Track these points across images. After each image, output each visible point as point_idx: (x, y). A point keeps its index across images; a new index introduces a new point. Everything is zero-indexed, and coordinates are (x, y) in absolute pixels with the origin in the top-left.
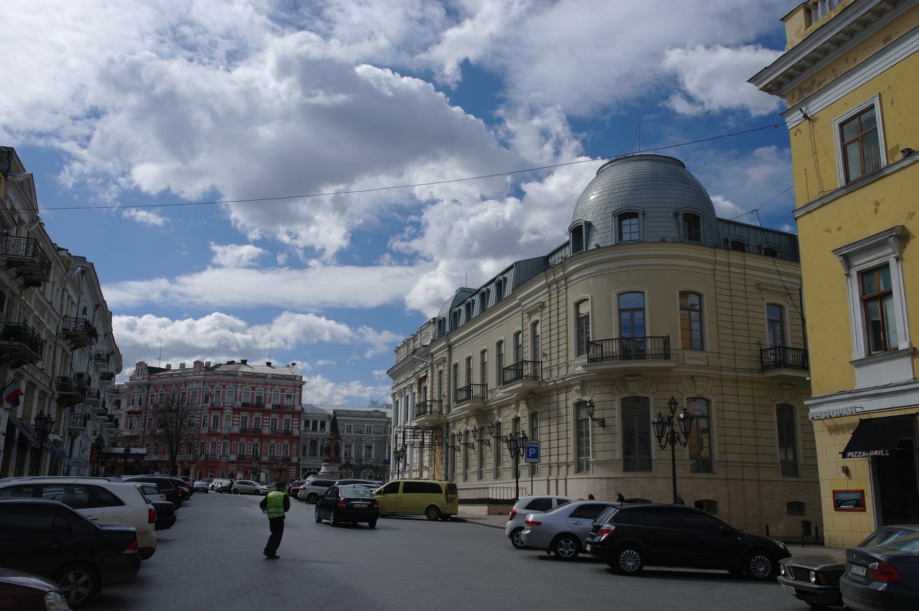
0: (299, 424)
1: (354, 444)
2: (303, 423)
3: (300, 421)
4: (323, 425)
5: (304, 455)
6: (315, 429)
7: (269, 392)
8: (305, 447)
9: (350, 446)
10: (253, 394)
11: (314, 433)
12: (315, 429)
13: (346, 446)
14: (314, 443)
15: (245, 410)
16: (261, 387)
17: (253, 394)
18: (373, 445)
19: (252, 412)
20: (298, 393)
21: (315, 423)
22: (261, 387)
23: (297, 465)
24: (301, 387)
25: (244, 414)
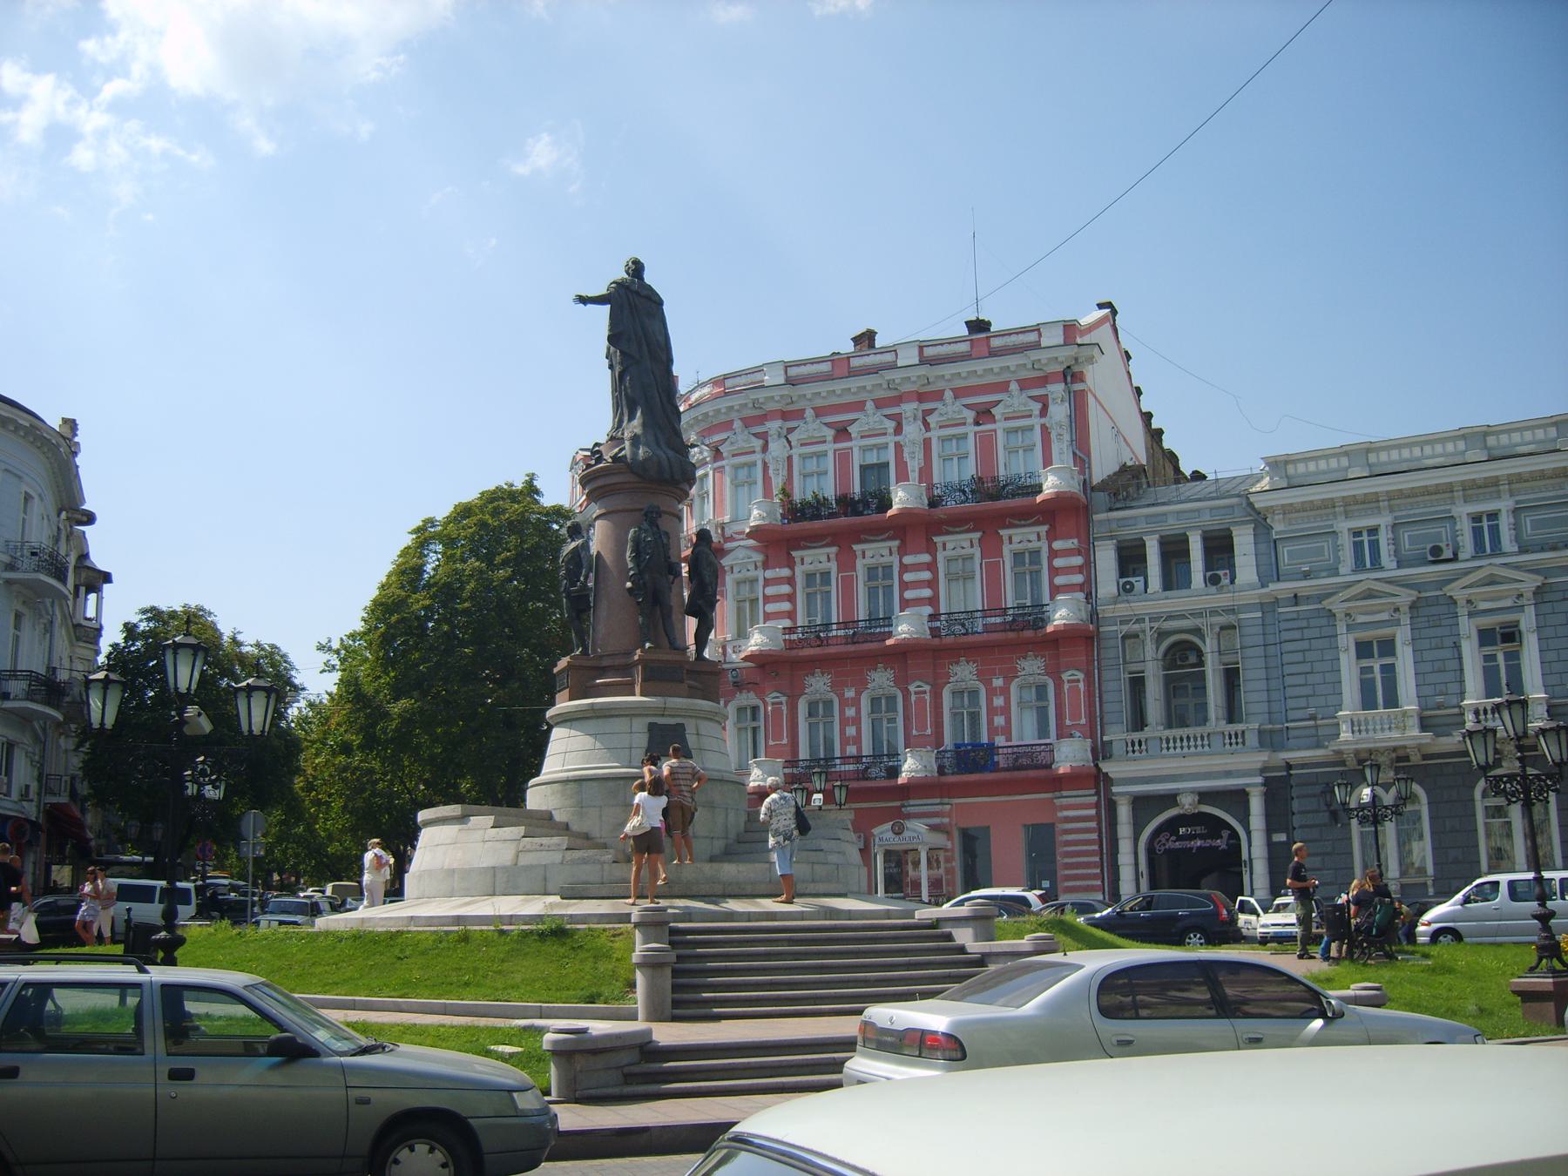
0: (1088, 567)
1: (1402, 635)
2: (1106, 559)
3: (1087, 551)
4: (1219, 548)
5: (1139, 722)
6: (1175, 577)
7: (912, 431)
8: (1137, 684)
9: (1388, 647)
10: (843, 459)
11: (1177, 601)
12: (1175, 577)
13: (1363, 649)
14: (1182, 655)
15: (813, 540)
16: (871, 419)
17: (843, 459)
18: (1527, 621)
19: (844, 541)
20: (1060, 412)
21: (1174, 551)
22: (871, 419)
23: (1096, 780)
24: (1071, 375)
25: (817, 559)
